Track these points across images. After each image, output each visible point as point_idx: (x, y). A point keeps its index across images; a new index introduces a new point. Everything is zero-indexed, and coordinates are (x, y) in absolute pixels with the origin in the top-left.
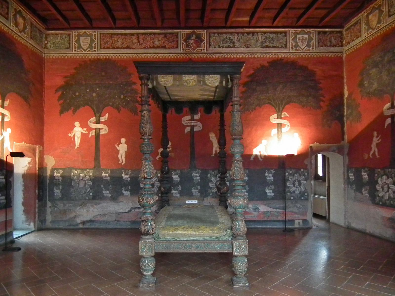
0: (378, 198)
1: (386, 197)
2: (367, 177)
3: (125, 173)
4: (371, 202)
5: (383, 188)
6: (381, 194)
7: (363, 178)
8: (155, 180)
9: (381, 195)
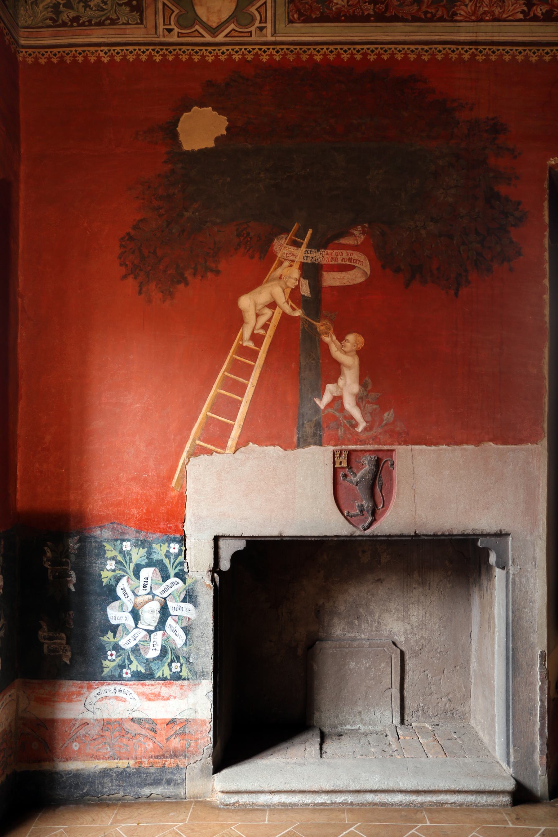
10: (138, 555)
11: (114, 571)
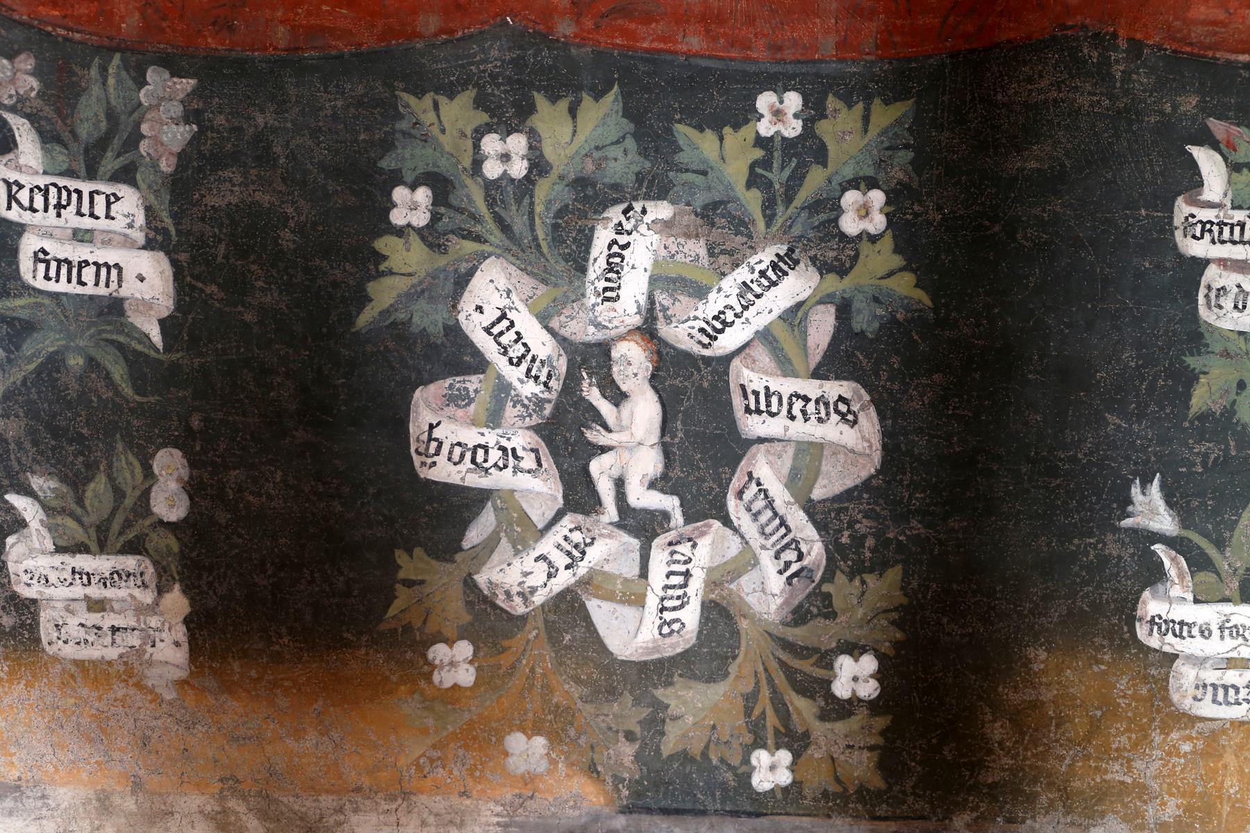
3: (48, 137)
8: (765, 336)
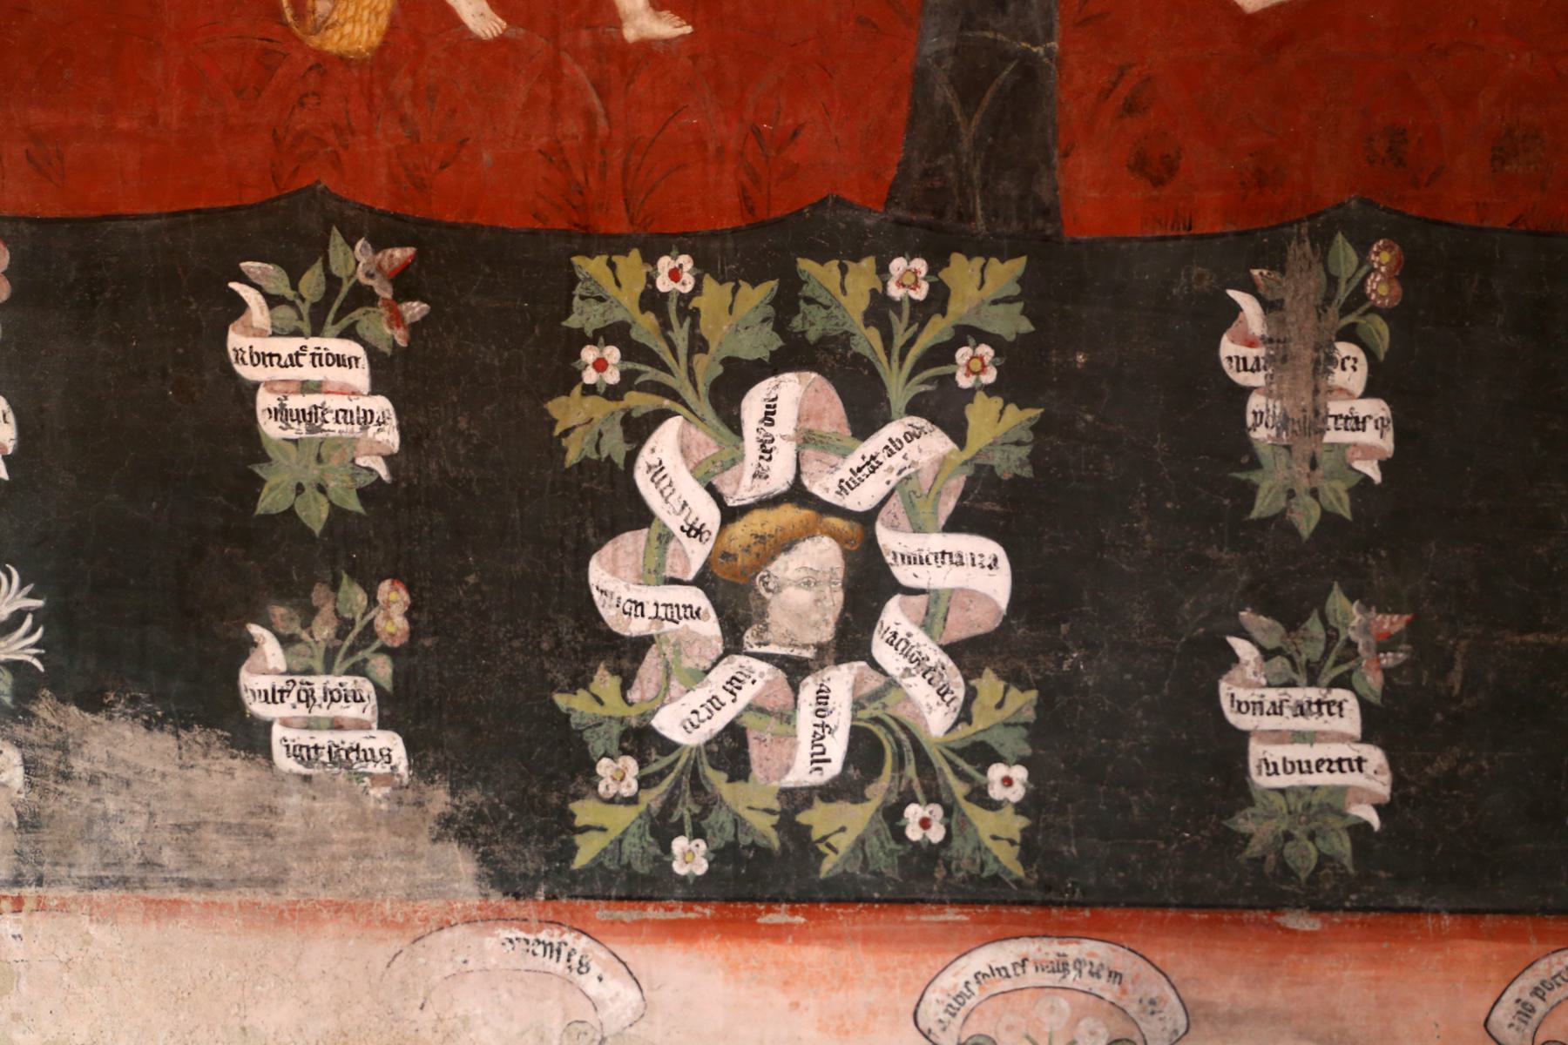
0: (617, 774)
1: (811, 749)
2: (381, 404)
4: (461, 864)
5: (734, 597)
6: (699, 696)
7: (271, 428)
9: (685, 720)
10: (736, 316)
11: (613, 393)
